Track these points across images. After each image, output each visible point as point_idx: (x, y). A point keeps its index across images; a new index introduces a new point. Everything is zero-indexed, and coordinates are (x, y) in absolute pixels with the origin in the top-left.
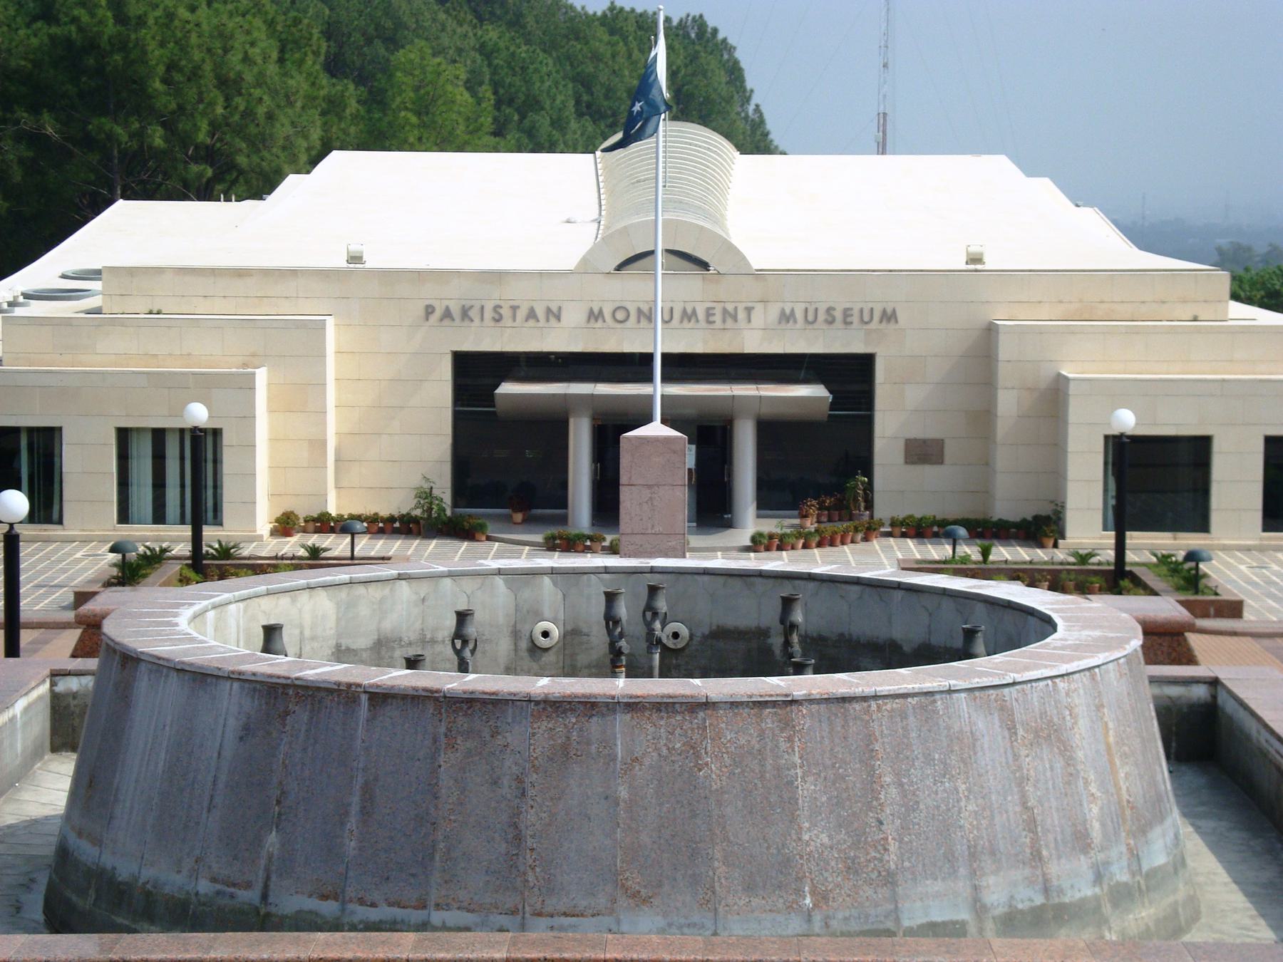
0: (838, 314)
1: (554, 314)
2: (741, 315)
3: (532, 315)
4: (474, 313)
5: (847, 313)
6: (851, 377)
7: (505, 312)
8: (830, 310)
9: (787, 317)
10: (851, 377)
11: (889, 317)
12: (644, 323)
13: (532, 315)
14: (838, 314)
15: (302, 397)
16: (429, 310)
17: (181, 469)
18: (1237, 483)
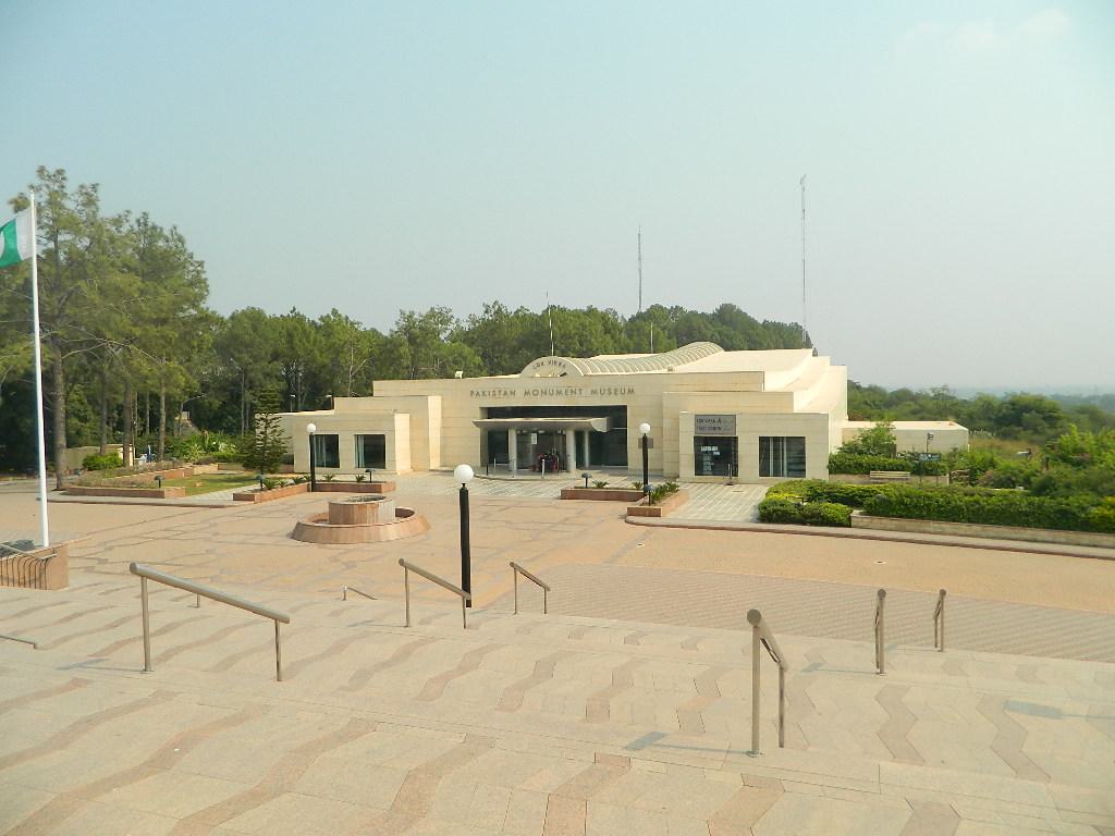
0: (613, 391)
1: (513, 393)
2: (578, 392)
3: (505, 394)
4: (487, 393)
5: (616, 390)
6: (617, 415)
7: (497, 393)
8: (609, 390)
9: (594, 392)
10: (617, 415)
11: (631, 391)
12: (544, 396)
13: (505, 394)
14: (613, 391)
15: (419, 426)
16: (472, 392)
17: (374, 451)
18: (748, 454)
